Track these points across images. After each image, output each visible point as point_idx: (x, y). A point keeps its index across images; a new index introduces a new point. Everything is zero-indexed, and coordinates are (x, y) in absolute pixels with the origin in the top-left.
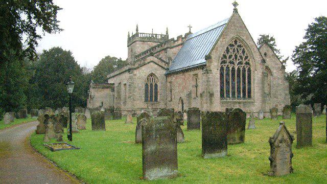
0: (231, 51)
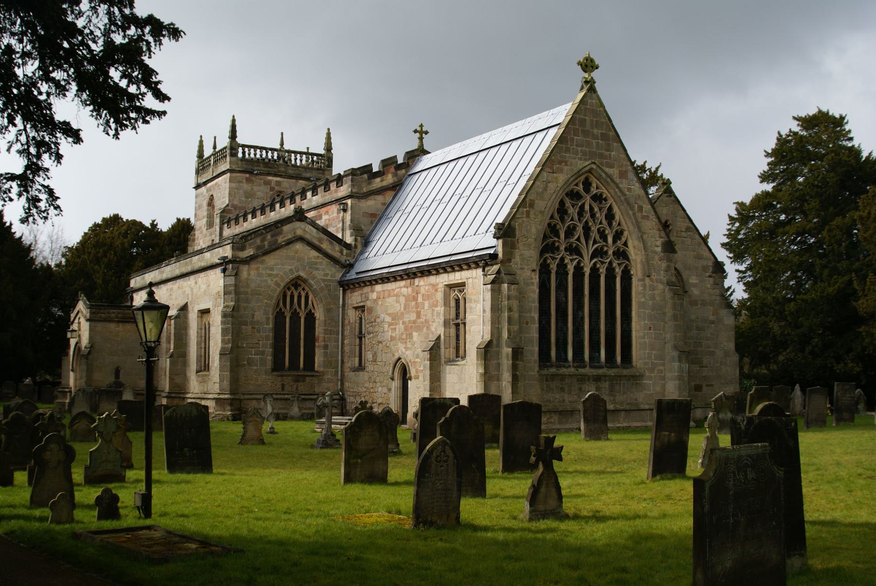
0: (573, 211)
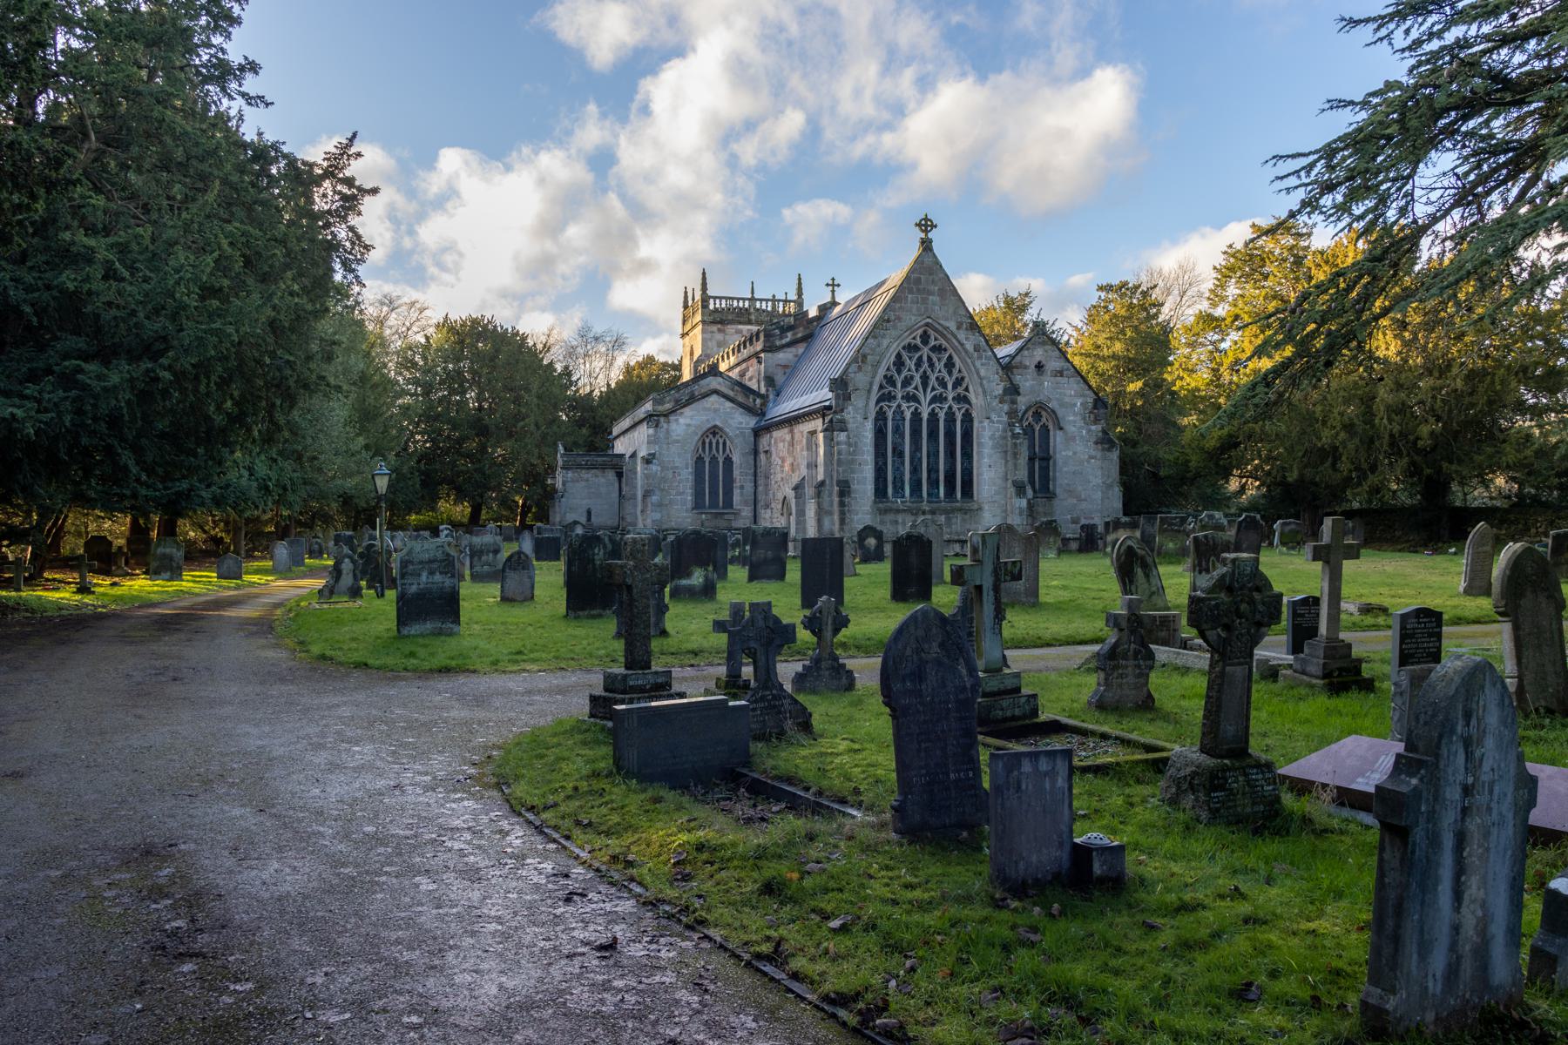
0: (910, 364)
